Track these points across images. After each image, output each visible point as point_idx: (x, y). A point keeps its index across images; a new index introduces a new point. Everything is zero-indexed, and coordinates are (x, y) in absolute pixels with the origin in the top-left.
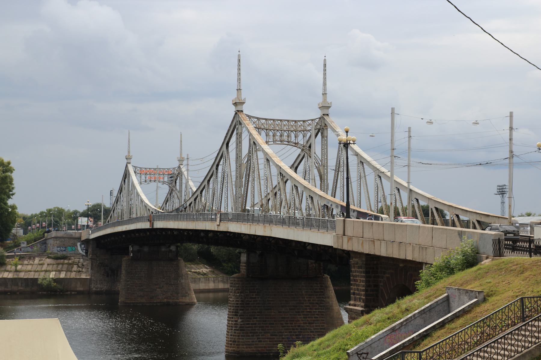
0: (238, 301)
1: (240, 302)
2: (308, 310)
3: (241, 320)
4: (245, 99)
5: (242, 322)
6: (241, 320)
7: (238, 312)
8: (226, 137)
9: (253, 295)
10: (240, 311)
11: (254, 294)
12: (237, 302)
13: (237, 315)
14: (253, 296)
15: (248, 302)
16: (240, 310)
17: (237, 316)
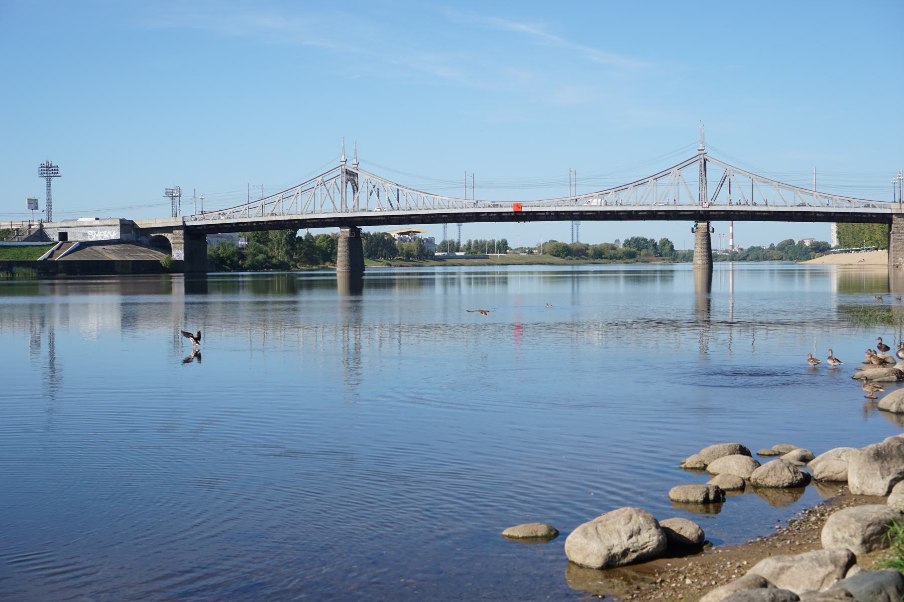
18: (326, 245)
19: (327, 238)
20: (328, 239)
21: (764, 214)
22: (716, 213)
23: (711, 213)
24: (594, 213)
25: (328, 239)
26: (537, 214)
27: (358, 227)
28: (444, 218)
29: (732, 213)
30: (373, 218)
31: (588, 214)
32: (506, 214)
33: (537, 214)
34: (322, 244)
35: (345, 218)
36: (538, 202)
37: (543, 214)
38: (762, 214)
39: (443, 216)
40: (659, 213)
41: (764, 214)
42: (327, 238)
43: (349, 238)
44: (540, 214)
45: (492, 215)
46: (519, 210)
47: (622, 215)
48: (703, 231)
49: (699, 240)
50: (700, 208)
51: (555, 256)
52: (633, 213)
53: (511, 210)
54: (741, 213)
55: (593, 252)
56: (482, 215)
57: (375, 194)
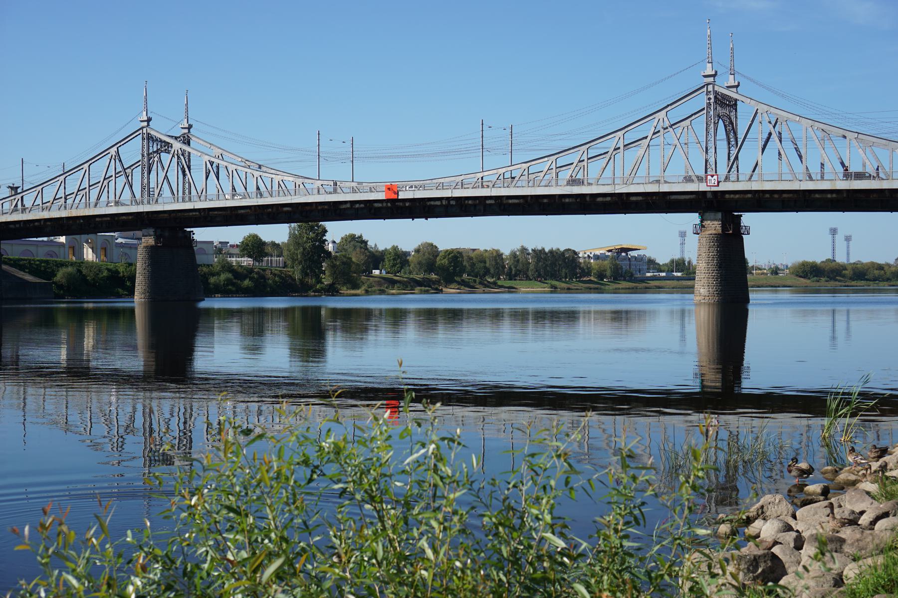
8: (668, 106)
18: (447, 262)
19: (449, 254)
20: (450, 256)
21: (829, 196)
22: (737, 196)
23: (727, 196)
24: (522, 201)
25: (450, 256)
26: (428, 203)
27: (188, 230)
28: (288, 212)
29: (767, 196)
30: (191, 214)
31: (510, 201)
32: (380, 205)
33: (428, 203)
34: (443, 262)
35: (148, 213)
36: (430, 181)
37: (438, 203)
38: (824, 196)
39: (286, 209)
40: (633, 199)
41: (829, 196)
42: (449, 254)
43: (152, 247)
44: (432, 203)
45: (357, 206)
46: (394, 196)
47: (569, 204)
48: (714, 232)
49: (703, 250)
50: (703, 187)
51: (801, 277)
52: (588, 198)
53: (381, 196)
54: (785, 196)
55: (851, 273)
56: (344, 206)
57: (212, 175)
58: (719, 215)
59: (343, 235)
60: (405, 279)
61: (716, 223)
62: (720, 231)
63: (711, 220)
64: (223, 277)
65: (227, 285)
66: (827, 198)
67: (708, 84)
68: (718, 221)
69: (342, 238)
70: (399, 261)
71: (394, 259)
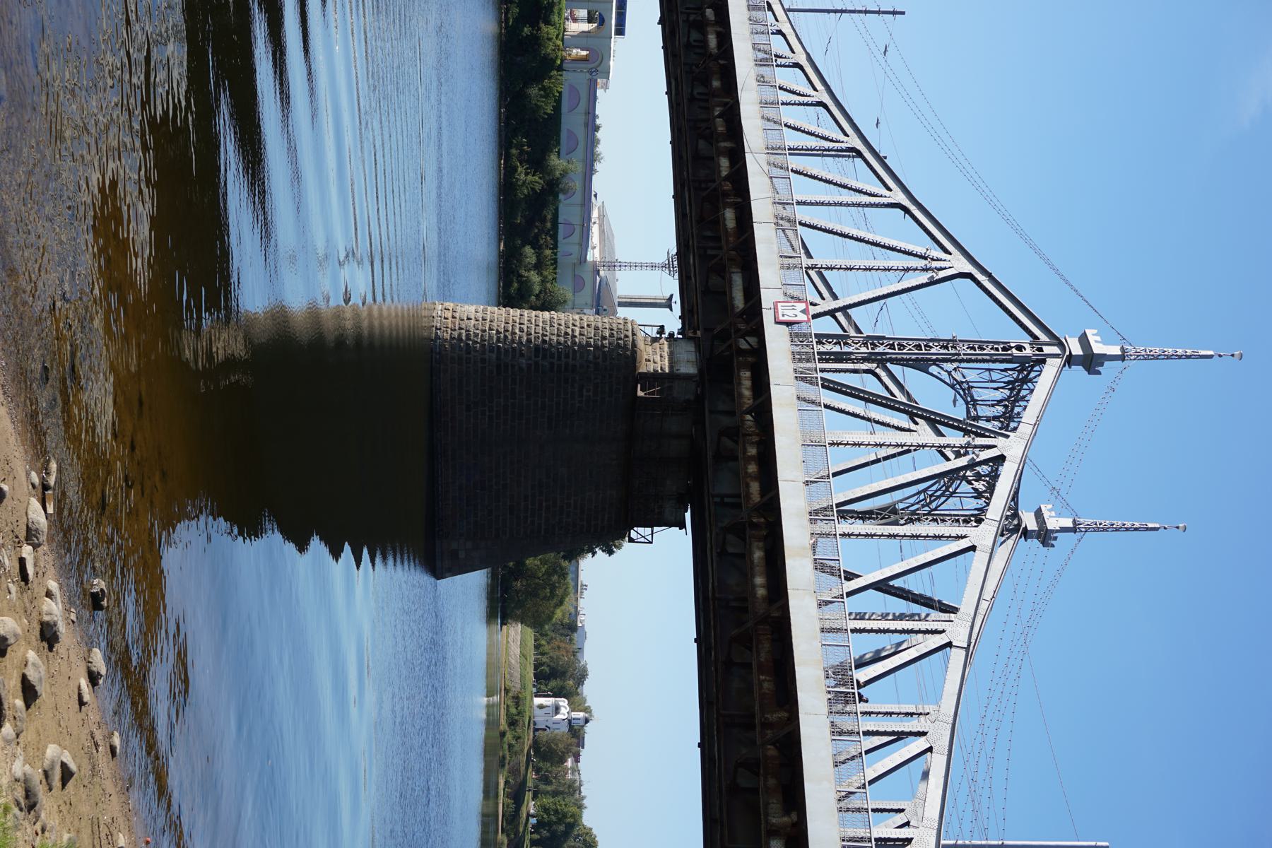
0: (574, 359)
1: (571, 361)
2: (544, 504)
3: (524, 366)
4: (1099, 373)
5: (521, 369)
6: (524, 366)
7: (544, 357)
8: (989, 275)
9: (588, 391)
10: (546, 364)
11: (591, 394)
12: (571, 356)
13: (536, 356)
14: (584, 390)
15: (570, 380)
16: (552, 364)
17: (536, 357)
58: (688, 368)
59: (595, 832)
60: (521, 830)
61: (666, 362)
62: (642, 369)
63: (671, 355)
64: (535, 277)
65: (521, 283)
66: (753, 576)
67: (1061, 344)
68: (671, 367)
69: (591, 829)
70: (554, 819)
71: (556, 811)
